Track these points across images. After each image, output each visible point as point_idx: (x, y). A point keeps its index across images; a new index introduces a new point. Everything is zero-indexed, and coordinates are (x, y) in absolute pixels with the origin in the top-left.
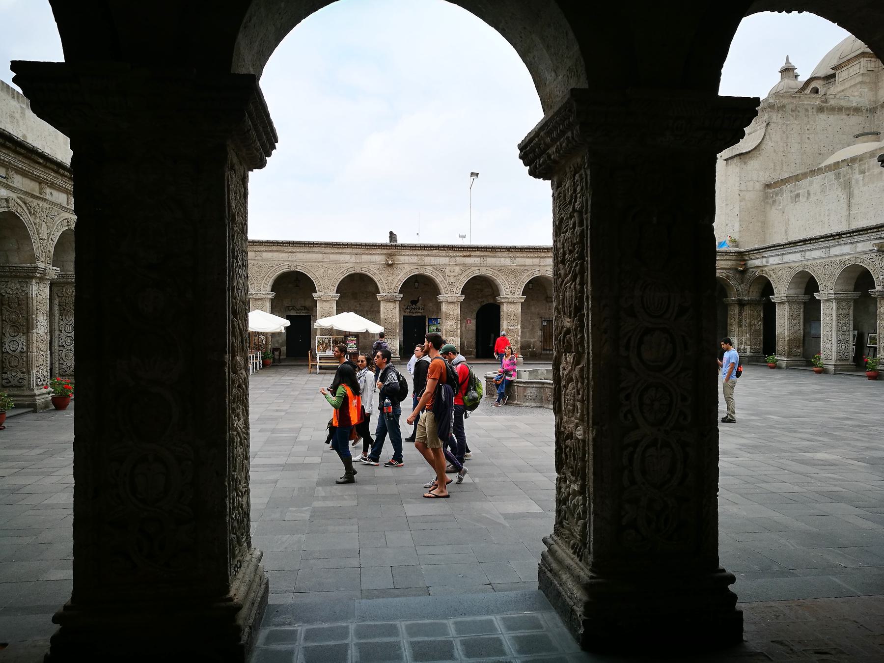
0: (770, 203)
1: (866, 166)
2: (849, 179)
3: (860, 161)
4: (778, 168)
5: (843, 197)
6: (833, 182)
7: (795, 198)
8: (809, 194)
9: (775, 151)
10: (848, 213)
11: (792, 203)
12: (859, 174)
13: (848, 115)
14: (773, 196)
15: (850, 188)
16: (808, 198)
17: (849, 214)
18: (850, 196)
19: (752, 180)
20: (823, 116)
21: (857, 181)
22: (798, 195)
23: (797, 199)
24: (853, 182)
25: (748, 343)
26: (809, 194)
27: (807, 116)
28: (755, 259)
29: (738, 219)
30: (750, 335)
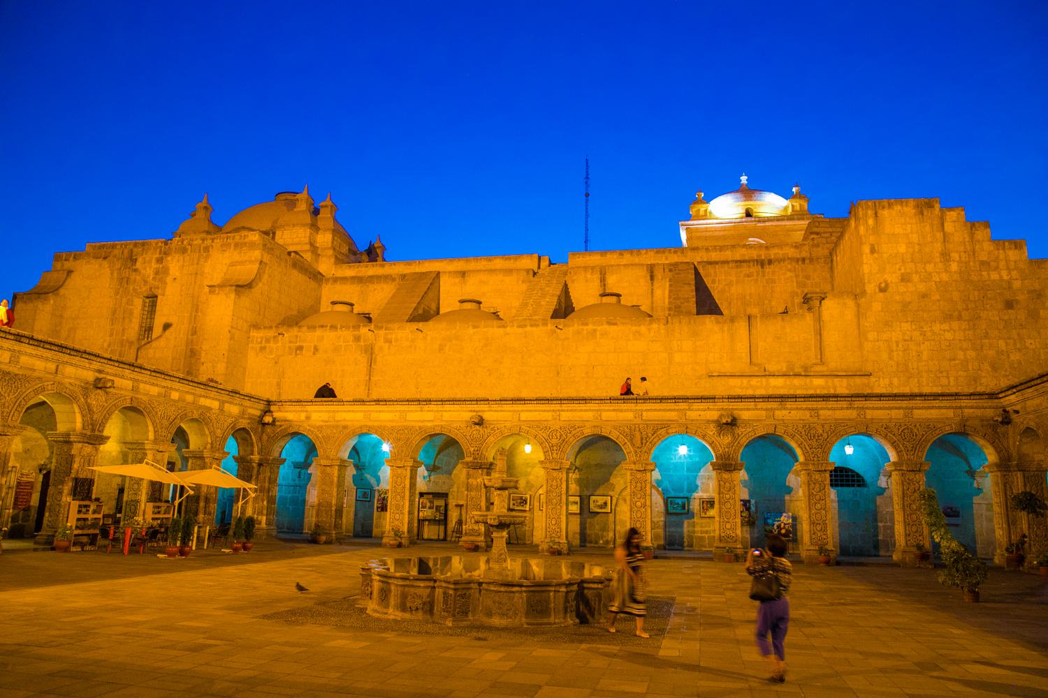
0: (256, 350)
1: (394, 336)
2: (372, 344)
3: (386, 329)
4: (262, 313)
5: (363, 360)
6: (351, 343)
7: (296, 351)
8: (316, 349)
9: (261, 293)
10: (368, 378)
11: (290, 354)
12: (385, 343)
13: (310, 278)
14: (261, 343)
15: (372, 354)
16: (314, 354)
17: (370, 379)
18: (371, 363)
19: (242, 318)
20: (295, 272)
21: (381, 349)
22: (301, 348)
23: (298, 352)
24: (376, 349)
25: (265, 512)
26: (316, 349)
27: (286, 266)
28: (287, 411)
29: (225, 360)
30: (268, 502)
